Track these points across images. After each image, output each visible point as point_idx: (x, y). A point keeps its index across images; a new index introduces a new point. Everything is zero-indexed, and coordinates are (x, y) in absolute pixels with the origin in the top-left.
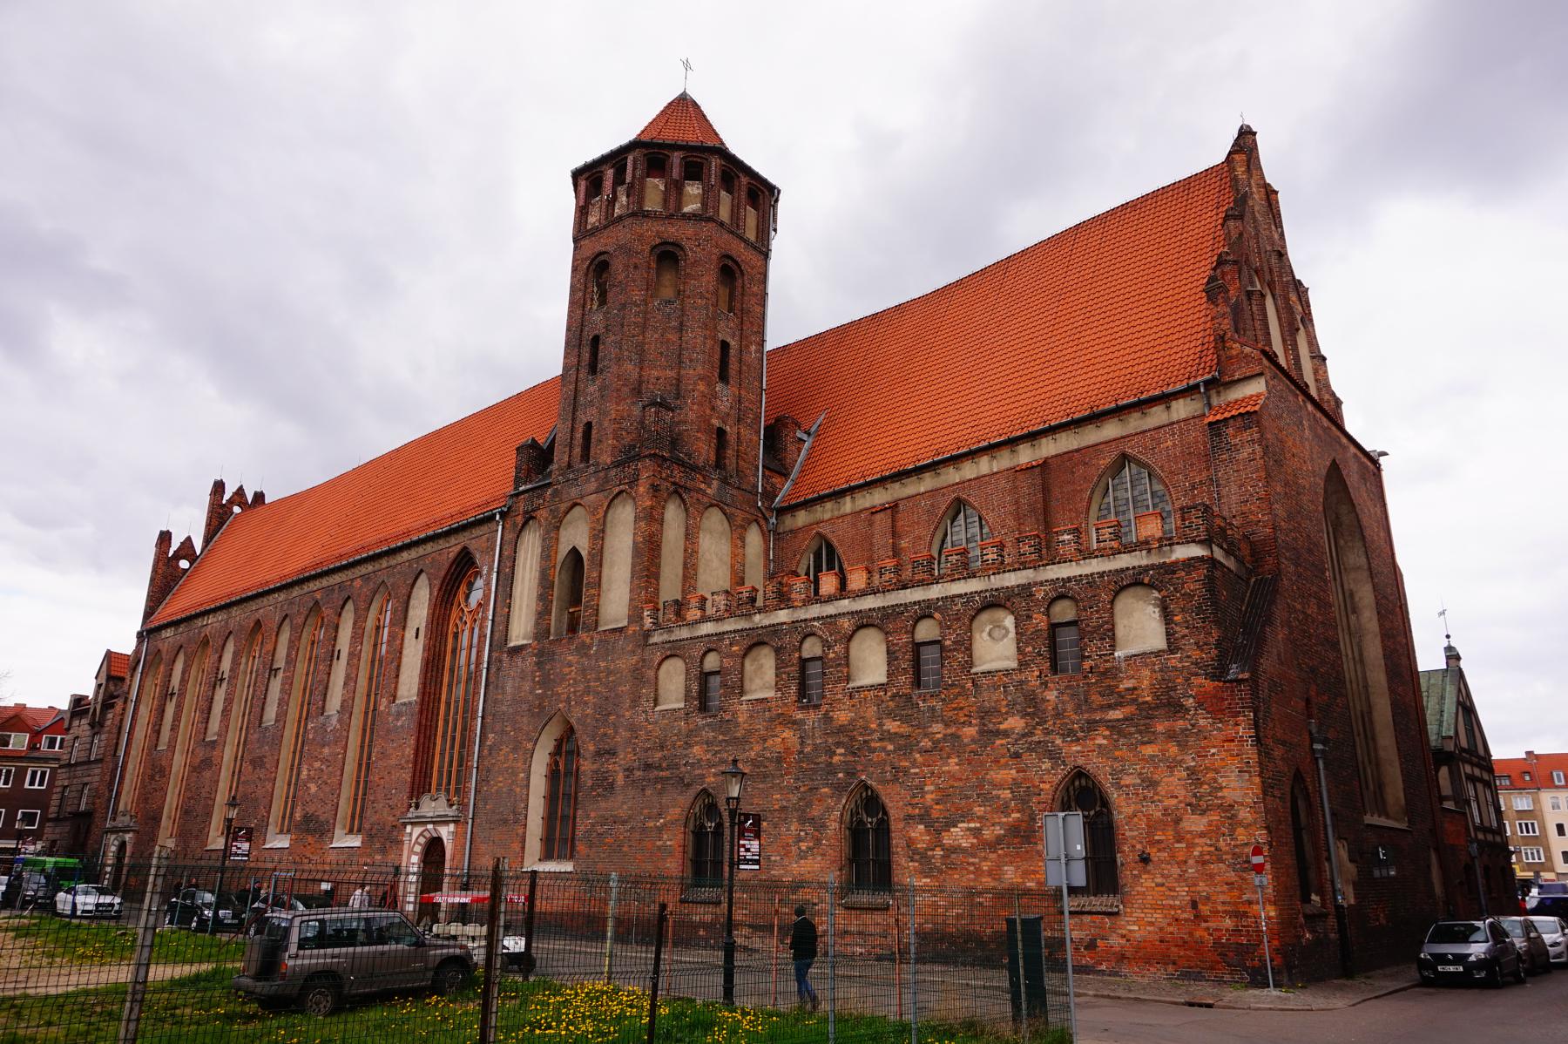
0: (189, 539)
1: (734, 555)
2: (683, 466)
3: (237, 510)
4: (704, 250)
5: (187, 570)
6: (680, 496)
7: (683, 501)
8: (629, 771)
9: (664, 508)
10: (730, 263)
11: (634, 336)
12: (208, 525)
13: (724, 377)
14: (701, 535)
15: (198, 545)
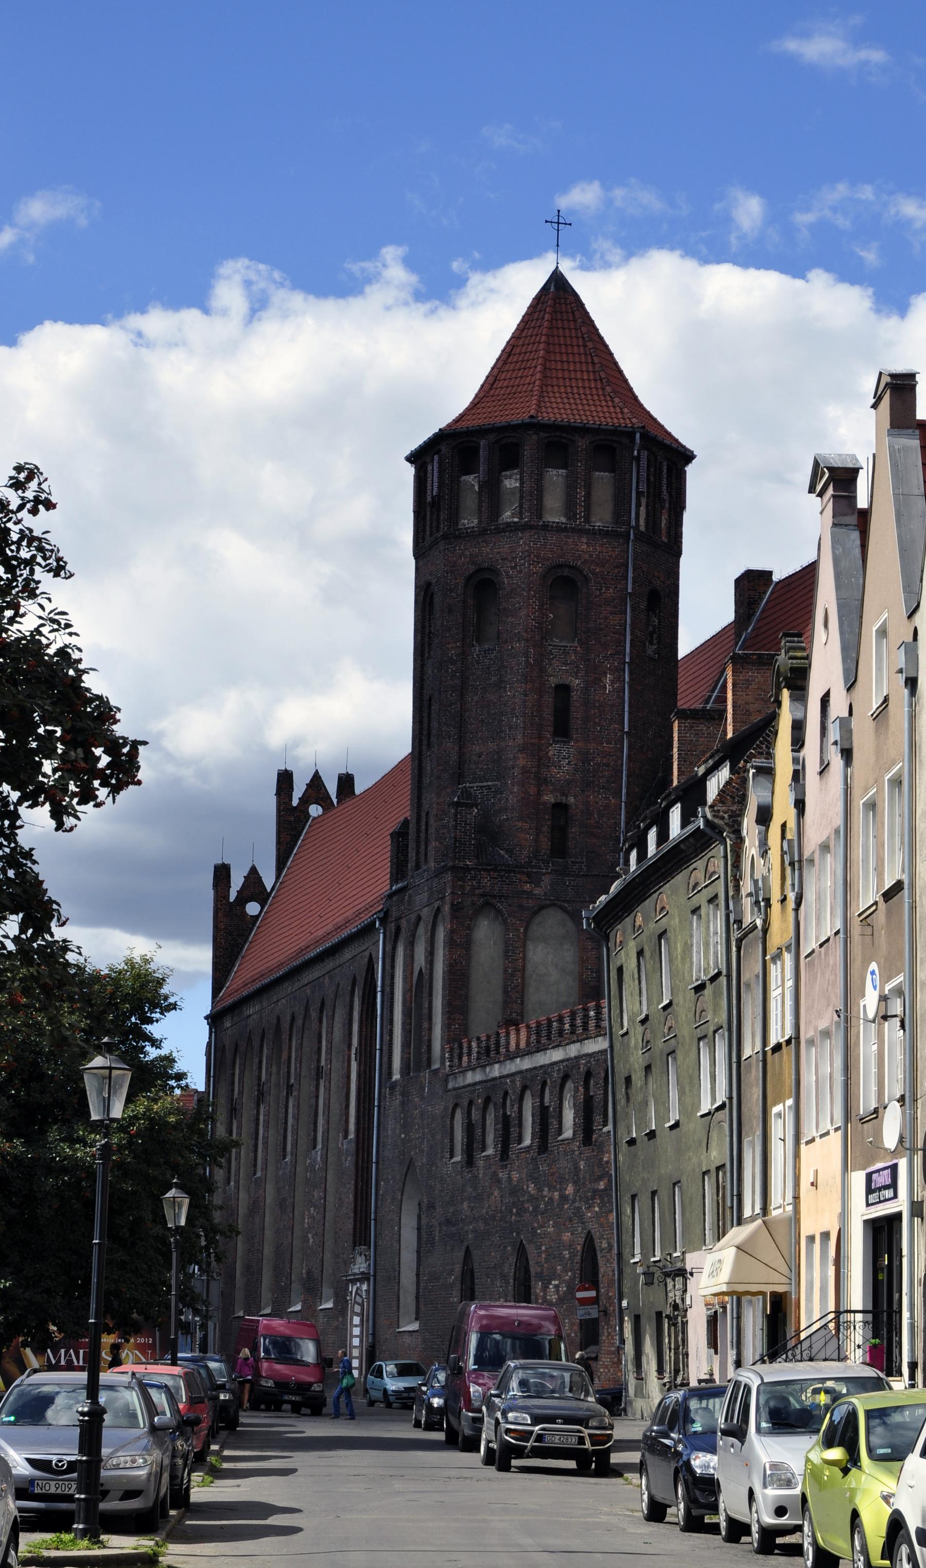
0: (253, 870)
1: (582, 962)
2: (495, 870)
3: (315, 810)
4: (520, 572)
5: (257, 917)
6: (493, 906)
7: (499, 912)
8: (440, 1225)
9: (469, 928)
10: (566, 572)
11: (451, 704)
12: (279, 842)
13: (562, 730)
14: (530, 946)
15: (269, 881)
